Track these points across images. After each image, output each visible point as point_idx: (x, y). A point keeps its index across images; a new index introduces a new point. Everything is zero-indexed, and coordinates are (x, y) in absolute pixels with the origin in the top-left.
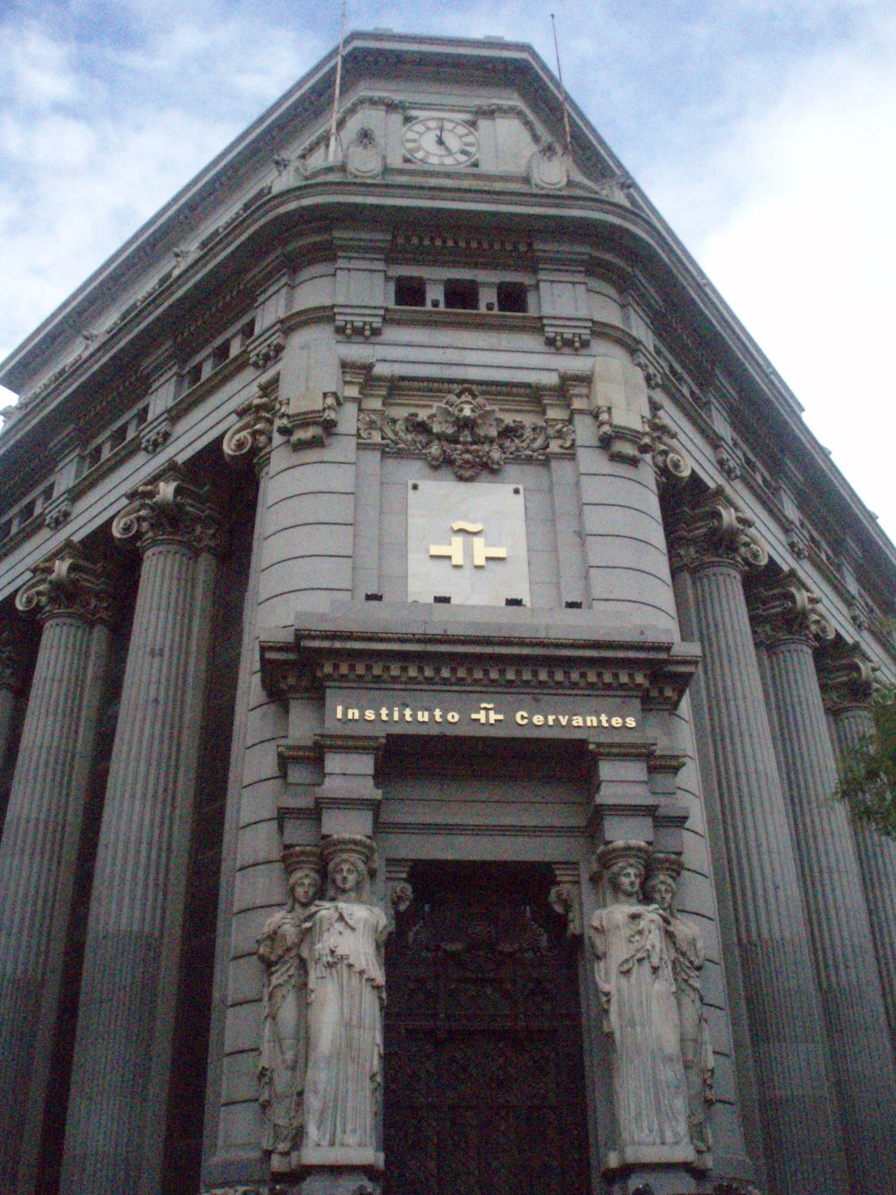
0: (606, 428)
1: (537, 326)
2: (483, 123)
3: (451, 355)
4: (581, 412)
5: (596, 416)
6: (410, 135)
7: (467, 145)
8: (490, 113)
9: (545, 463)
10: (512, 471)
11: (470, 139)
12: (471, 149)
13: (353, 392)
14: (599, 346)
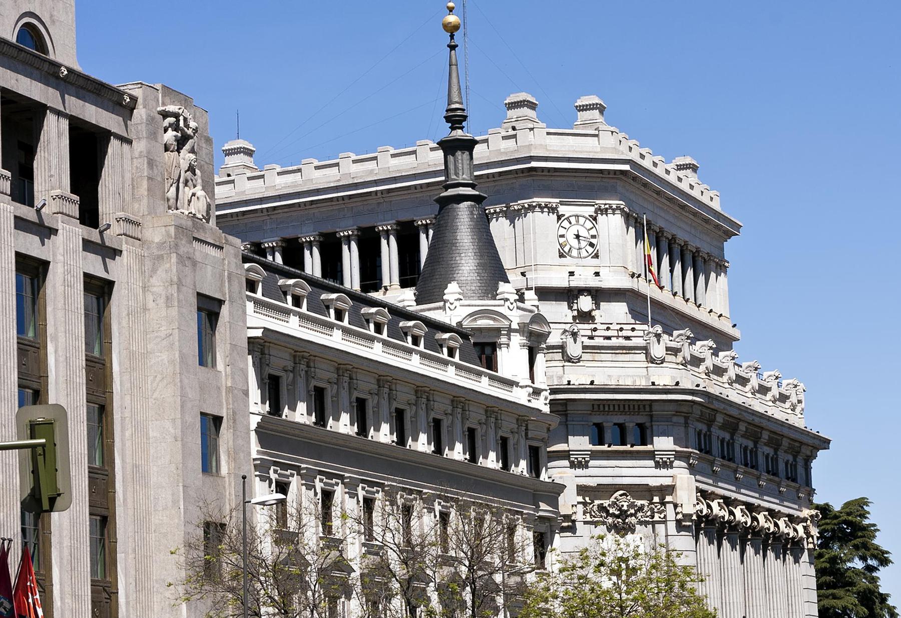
0: (680, 516)
1: (651, 455)
2: (600, 218)
3: (617, 472)
4: (669, 502)
5: (676, 506)
6: (562, 231)
7: (593, 237)
8: (604, 212)
9: (653, 524)
10: (638, 527)
11: (593, 232)
12: (594, 241)
13: (580, 499)
14: (677, 463)
